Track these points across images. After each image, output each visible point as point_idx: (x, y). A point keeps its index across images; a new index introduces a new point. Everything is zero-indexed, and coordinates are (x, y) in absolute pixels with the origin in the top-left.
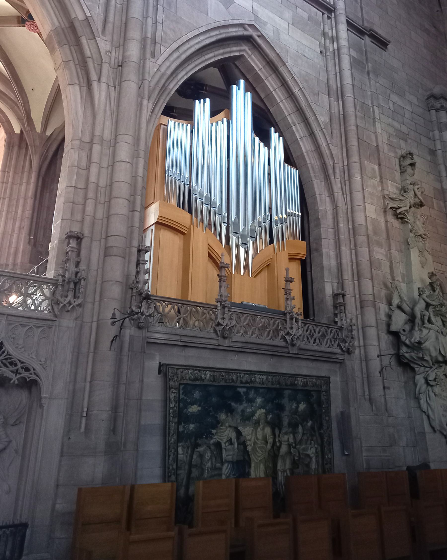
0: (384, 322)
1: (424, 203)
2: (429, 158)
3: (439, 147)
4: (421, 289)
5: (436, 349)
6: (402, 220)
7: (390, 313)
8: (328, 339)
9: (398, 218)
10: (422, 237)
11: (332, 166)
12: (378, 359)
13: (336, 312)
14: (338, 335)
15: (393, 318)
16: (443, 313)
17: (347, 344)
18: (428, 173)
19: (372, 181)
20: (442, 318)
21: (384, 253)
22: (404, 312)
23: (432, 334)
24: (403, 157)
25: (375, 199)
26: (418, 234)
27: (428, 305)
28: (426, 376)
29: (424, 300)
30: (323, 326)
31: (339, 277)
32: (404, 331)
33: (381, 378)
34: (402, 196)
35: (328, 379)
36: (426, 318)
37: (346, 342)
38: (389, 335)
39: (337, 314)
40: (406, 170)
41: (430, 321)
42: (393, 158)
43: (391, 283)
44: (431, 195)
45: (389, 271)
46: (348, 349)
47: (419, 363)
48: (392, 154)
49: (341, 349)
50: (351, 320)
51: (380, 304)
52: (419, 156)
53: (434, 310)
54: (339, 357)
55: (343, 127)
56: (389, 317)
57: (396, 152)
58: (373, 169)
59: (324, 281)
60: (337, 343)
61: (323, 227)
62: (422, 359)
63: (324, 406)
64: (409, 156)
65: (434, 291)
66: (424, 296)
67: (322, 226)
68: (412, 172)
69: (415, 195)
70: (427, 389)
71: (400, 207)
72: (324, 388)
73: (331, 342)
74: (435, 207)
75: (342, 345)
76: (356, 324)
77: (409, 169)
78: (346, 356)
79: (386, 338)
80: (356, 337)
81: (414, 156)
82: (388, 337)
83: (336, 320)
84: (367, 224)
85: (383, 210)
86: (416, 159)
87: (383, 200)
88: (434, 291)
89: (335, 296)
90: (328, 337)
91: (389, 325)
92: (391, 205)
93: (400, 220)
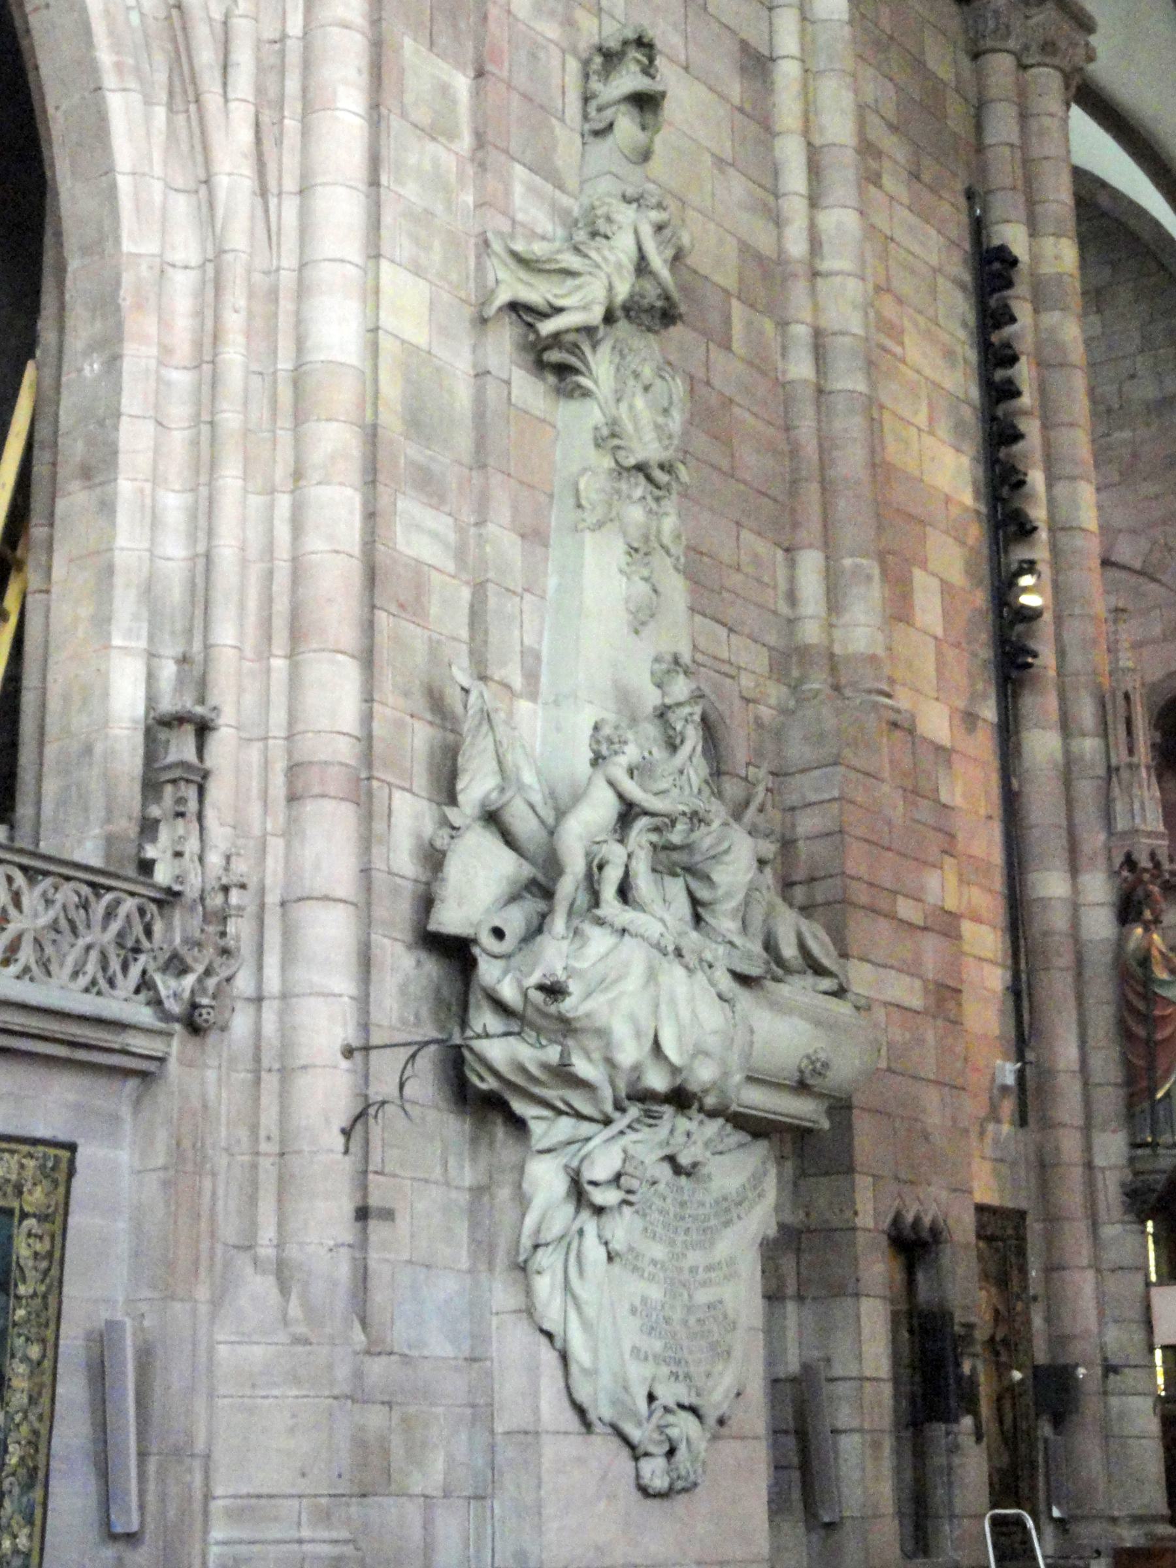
0: (409, 885)
1: (683, 308)
2: (735, 89)
3: (788, 41)
4: (607, 731)
5: (638, 1035)
6: (561, 379)
7: (438, 844)
8: (88, 948)
9: (540, 366)
10: (649, 479)
11: (219, 28)
12: (345, 1064)
13: (155, 811)
14: (148, 932)
15: (453, 869)
16: (698, 858)
17: (189, 980)
18: (720, 162)
19: (431, 147)
20: (695, 885)
21: (452, 537)
22: (509, 840)
24: (611, 58)
25: (437, 244)
26: (632, 461)
27: (628, 813)
28: (575, 1164)
29: (611, 784)
30: (68, 879)
31: (189, 631)
32: (498, 933)
33: (347, 1165)
34: (577, 250)
35: (65, 1154)
37: (184, 971)
38: (423, 955)
39: (157, 821)
40: (611, 126)
41: (624, 892)
42: (555, 53)
43: (466, 691)
44: (727, 278)
45: (464, 633)
46: (194, 1006)
47: (551, 1094)
48: (551, 30)
49: (156, 1002)
50: (228, 858)
51: (397, 795)
52: (686, 69)
53: (654, 837)
54: (139, 1043)
56: (434, 860)
57: (569, 22)
58: (444, 90)
59: (108, 647)
60: (135, 971)
61: (137, 356)
62: (563, 1075)
63: (22, 1290)
64: (634, 53)
65: (673, 747)
66: (618, 768)
68: (642, 137)
70: (575, 1227)
71: (559, 310)
72: (35, 1197)
73: (104, 964)
74: (736, 345)
75: (165, 985)
76: (253, 883)
77: (627, 125)
78: (177, 1045)
79: (404, 970)
80: (246, 950)
81: (659, 61)
82: (419, 963)
83: (150, 852)
84: (375, 368)
85: (468, 312)
86: (669, 78)
87: (478, 257)
88: (673, 747)
89: (159, 725)
90: (89, 939)
91: (427, 903)
92: (515, 286)
93: (551, 379)
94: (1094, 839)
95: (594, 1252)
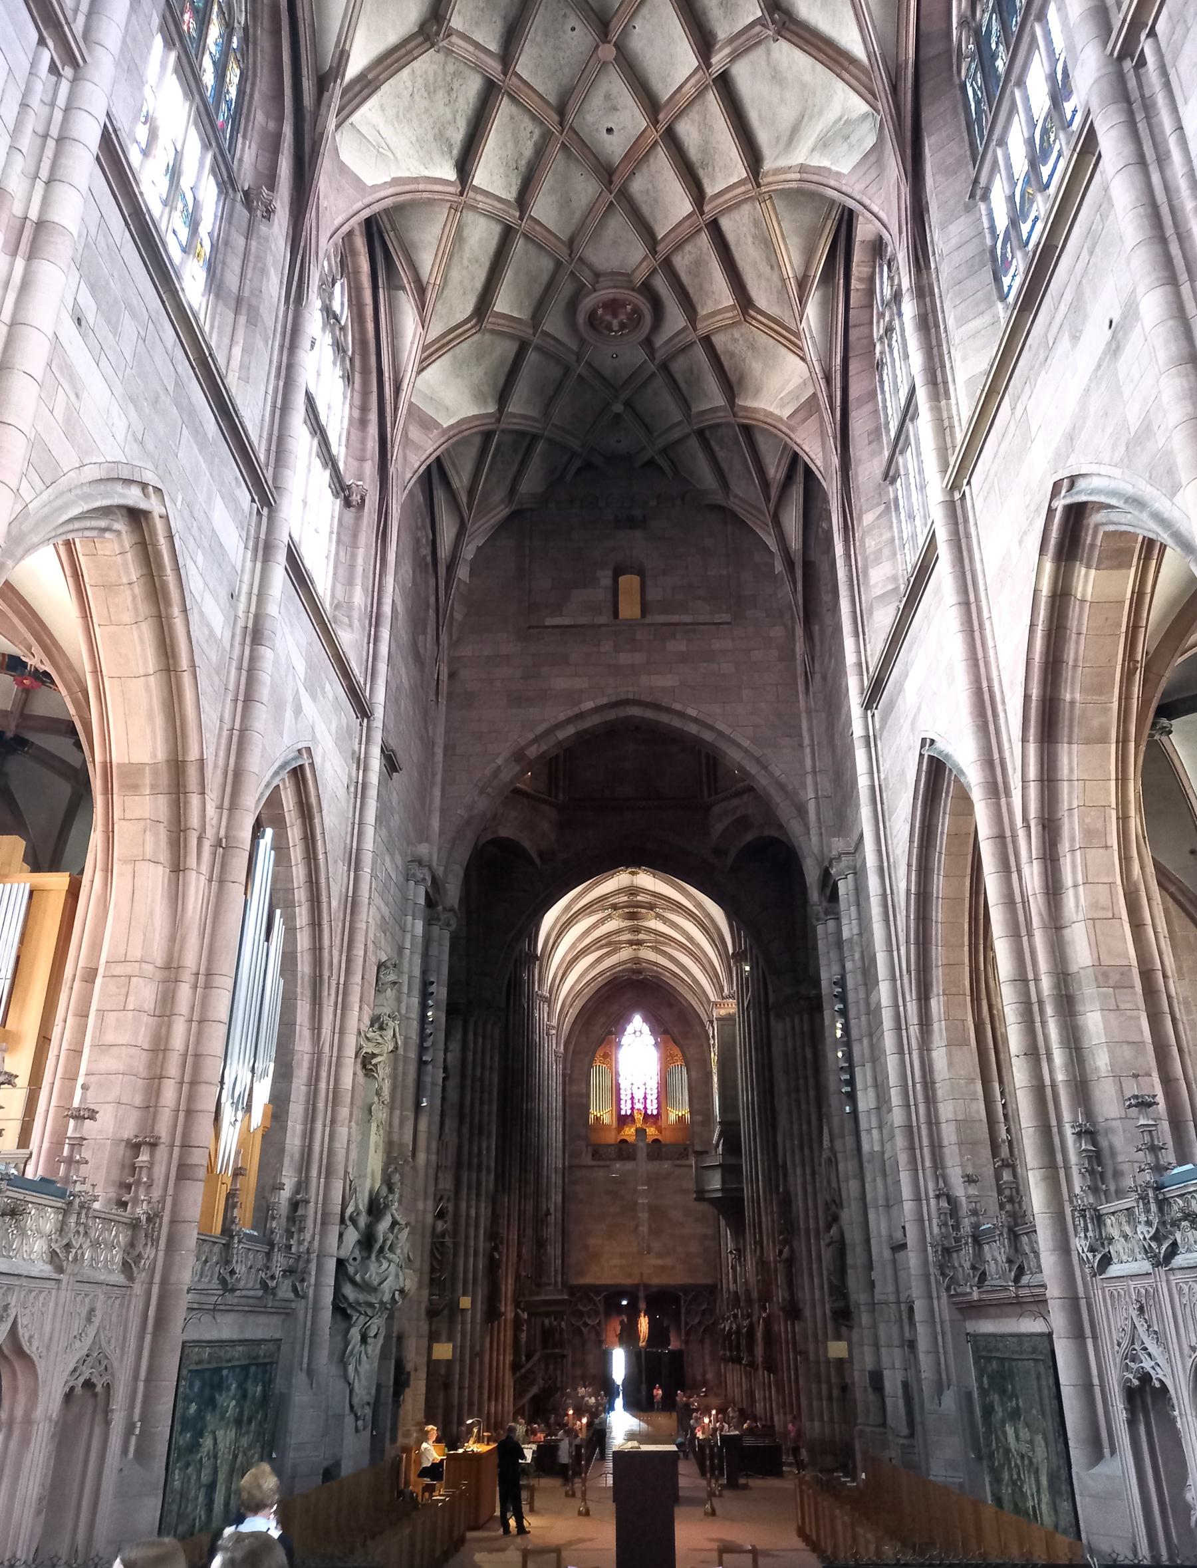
3: (408, 945)
23: (393, 1268)
36: (389, 1243)
55: (348, 918)
67: (294, 1080)
69: (394, 1035)
94: (432, 1189)
95: (364, 1357)
